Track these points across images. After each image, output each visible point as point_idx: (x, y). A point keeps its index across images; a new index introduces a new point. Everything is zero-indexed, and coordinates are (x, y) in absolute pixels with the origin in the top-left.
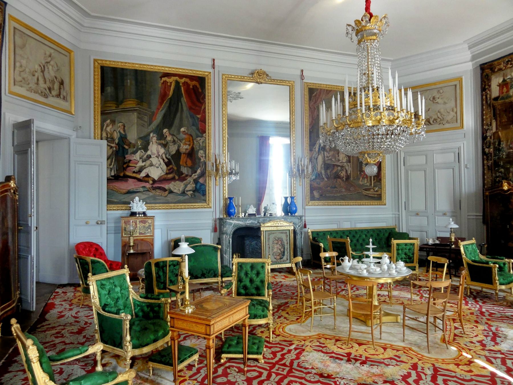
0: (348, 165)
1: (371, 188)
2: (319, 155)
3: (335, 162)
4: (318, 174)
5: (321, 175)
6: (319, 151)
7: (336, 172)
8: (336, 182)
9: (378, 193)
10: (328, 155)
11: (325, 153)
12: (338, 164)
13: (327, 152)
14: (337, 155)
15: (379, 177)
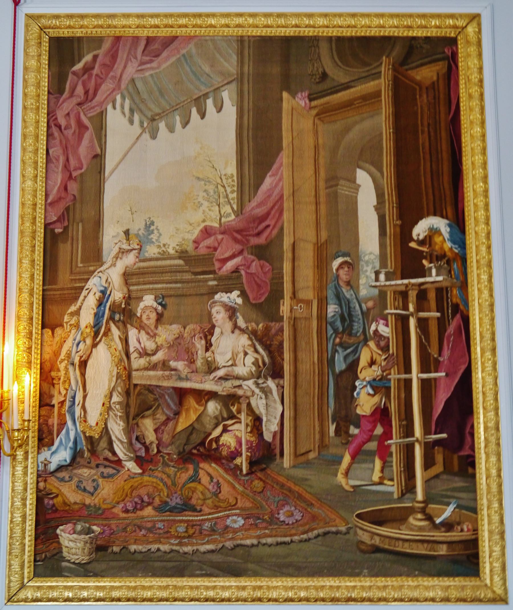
0: (266, 392)
1: (411, 511)
2: (95, 345)
3: (187, 379)
4: (90, 440)
5: (103, 444)
6: (96, 327)
7: (191, 429)
8: (195, 478)
9: (454, 535)
10: (150, 345)
11: (133, 333)
12: (209, 386)
13: (141, 327)
14: (200, 344)
15: (460, 446)
